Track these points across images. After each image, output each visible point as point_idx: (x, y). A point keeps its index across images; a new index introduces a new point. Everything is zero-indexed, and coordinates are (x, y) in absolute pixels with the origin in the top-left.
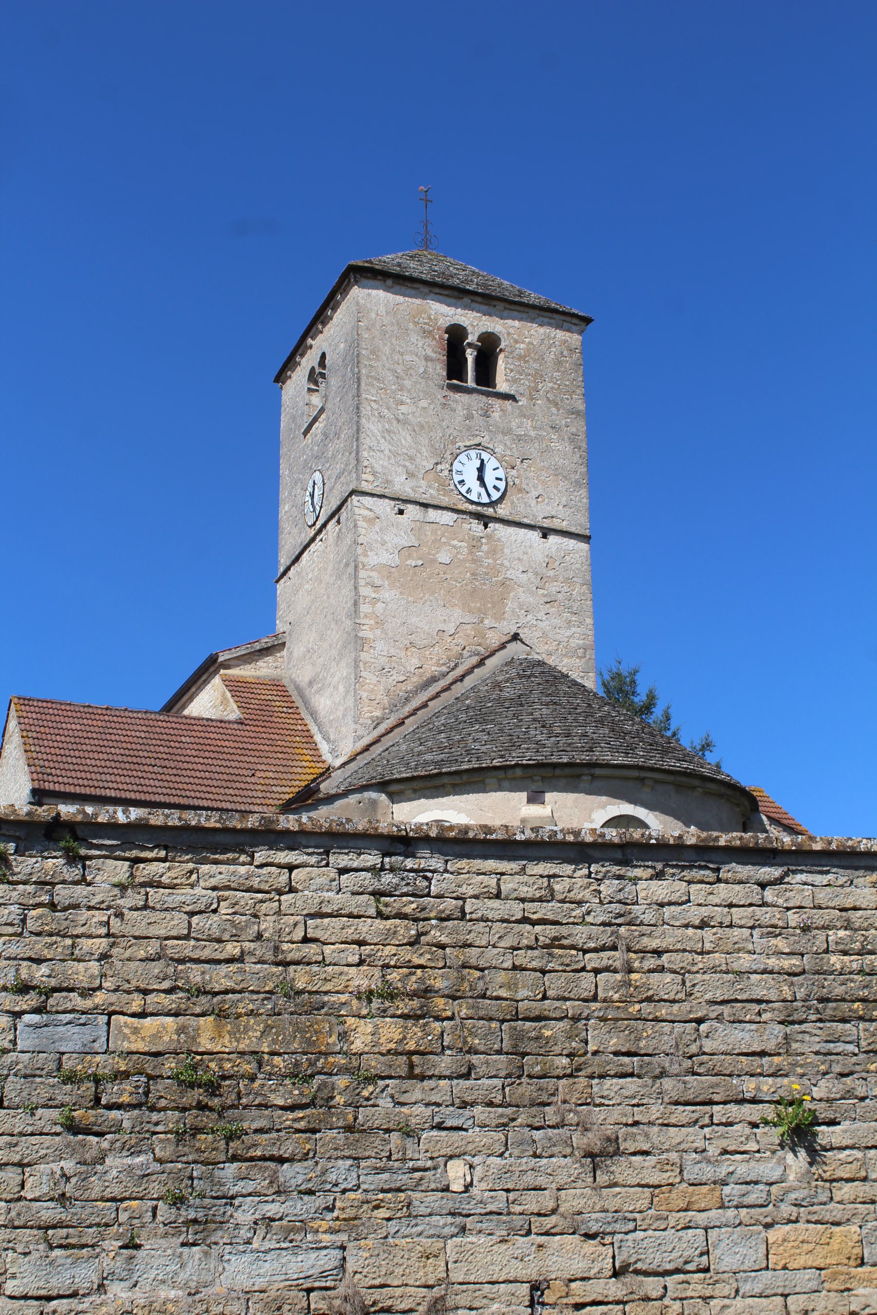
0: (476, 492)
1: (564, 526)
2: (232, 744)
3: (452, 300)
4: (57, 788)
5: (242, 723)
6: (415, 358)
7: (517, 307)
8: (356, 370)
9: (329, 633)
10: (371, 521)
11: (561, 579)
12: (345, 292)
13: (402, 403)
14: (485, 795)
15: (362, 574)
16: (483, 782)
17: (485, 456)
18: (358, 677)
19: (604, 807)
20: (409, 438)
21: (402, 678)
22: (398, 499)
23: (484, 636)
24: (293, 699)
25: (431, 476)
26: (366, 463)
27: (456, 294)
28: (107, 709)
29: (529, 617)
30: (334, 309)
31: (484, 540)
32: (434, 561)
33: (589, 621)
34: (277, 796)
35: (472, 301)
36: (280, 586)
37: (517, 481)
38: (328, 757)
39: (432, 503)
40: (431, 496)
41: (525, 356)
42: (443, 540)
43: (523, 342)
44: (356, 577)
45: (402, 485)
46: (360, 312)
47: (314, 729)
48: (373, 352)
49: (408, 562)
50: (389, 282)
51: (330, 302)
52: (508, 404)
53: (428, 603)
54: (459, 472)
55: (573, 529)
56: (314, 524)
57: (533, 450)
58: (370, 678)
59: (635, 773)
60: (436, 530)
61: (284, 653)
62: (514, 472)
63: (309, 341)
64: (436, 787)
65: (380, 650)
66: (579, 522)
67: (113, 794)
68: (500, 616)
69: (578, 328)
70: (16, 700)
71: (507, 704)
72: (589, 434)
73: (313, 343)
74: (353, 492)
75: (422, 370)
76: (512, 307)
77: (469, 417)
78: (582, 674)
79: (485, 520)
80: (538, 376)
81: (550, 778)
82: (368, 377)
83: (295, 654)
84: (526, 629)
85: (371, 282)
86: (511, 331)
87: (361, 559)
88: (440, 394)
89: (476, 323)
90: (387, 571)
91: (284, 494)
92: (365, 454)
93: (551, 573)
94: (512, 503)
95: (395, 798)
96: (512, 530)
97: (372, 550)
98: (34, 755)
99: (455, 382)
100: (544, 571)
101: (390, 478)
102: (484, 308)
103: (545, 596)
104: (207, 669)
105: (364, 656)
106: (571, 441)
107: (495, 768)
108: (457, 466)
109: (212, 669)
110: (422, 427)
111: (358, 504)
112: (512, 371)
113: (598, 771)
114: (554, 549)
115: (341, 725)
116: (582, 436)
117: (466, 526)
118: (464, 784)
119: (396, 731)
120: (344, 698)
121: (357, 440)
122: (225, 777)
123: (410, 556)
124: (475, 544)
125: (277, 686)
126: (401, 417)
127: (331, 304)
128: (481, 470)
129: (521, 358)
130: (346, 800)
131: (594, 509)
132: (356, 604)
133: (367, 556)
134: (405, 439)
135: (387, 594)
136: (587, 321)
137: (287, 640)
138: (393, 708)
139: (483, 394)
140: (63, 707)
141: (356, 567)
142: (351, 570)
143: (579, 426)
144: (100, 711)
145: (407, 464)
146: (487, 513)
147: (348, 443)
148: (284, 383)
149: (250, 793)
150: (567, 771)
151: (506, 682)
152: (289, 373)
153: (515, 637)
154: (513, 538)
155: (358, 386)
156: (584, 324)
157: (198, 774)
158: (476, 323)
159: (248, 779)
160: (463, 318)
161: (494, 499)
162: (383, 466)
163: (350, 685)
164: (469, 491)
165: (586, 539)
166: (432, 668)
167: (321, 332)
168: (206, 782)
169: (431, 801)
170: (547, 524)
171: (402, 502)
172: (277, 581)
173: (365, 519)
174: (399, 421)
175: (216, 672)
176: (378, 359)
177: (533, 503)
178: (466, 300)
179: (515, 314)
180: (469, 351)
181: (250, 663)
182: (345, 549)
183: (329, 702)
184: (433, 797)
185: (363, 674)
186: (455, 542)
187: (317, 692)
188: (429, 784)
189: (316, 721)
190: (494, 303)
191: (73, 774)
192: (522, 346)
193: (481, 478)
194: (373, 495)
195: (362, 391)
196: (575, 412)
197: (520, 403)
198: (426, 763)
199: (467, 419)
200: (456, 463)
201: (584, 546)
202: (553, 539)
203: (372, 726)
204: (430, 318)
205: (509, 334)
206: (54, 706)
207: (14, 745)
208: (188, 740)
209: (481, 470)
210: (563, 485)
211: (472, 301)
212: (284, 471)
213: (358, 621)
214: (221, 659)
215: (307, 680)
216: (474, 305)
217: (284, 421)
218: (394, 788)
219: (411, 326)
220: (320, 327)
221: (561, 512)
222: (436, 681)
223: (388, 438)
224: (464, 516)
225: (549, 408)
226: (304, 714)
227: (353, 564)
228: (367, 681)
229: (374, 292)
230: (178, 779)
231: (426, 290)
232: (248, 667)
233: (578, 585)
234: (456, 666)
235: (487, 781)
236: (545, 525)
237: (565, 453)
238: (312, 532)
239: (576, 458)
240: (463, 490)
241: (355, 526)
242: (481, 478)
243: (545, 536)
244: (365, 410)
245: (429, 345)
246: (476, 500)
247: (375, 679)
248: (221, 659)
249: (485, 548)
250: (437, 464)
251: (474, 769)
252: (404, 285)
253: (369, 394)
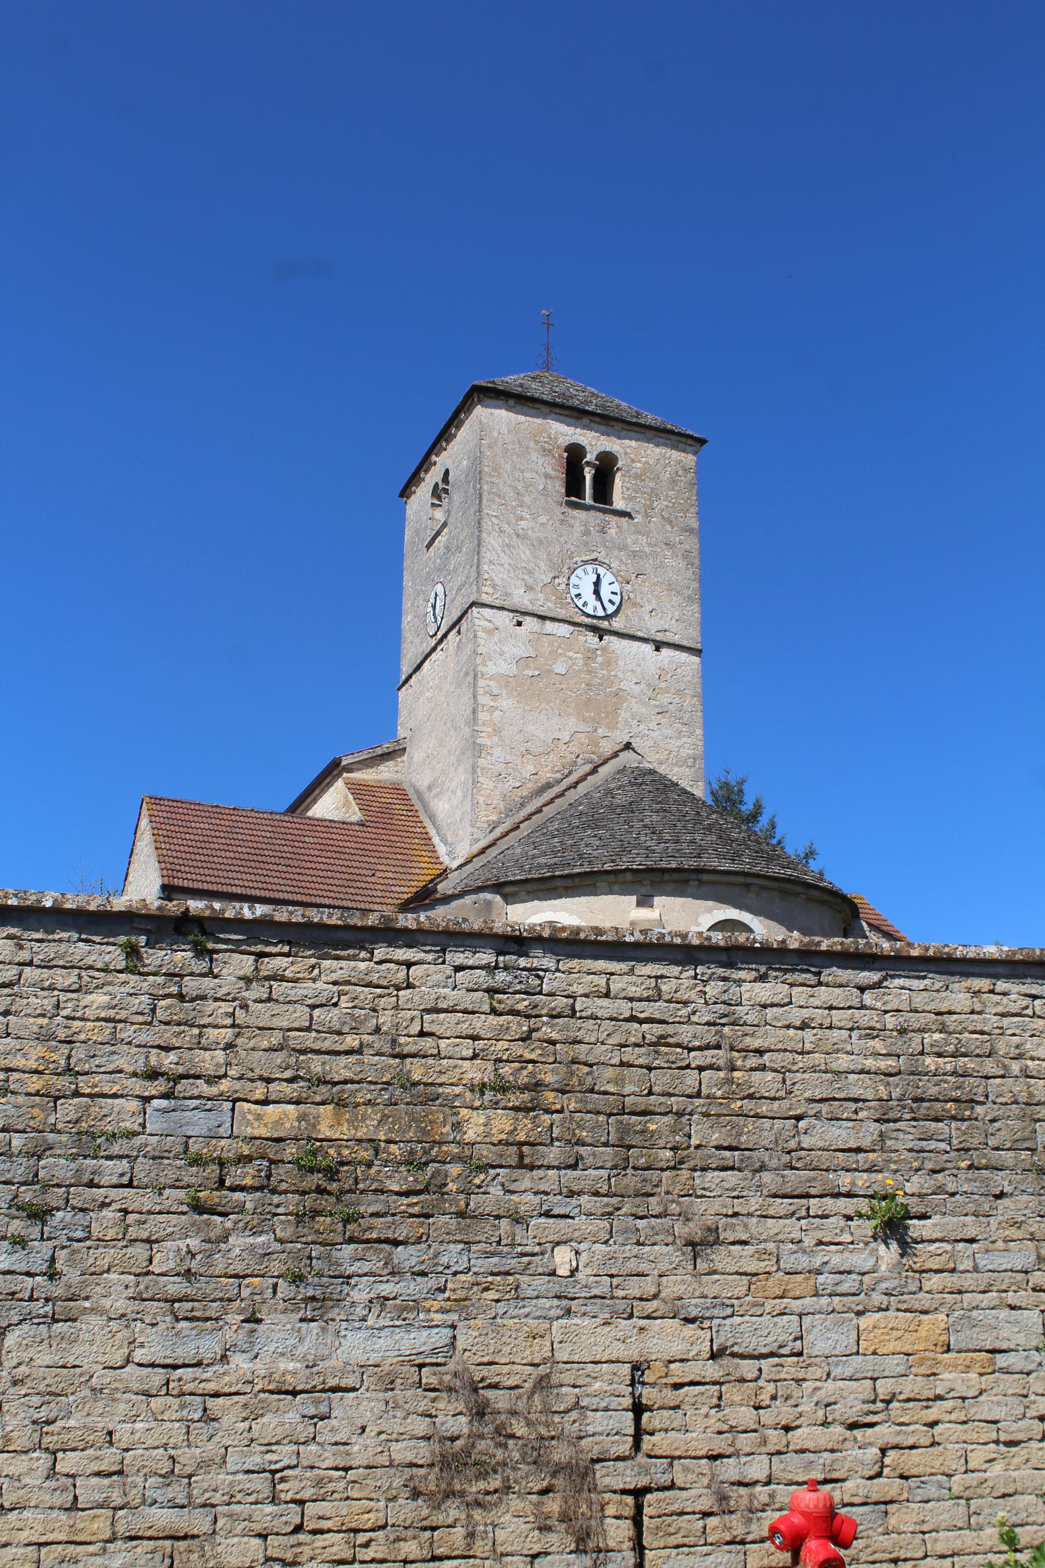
0: (592, 606)
1: (676, 639)
2: (353, 845)
3: (572, 420)
4: (186, 884)
5: (363, 825)
6: (535, 475)
7: (633, 428)
8: (478, 486)
9: (448, 739)
10: (490, 632)
11: (672, 690)
12: (469, 411)
13: (522, 519)
14: (596, 898)
15: (481, 683)
16: (594, 885)
17: (601, 571)
18: (475, 782)
19: (710, 911)
20: (528, 553)
21: (518, 784)
22: (517, 611)
23: (597, 745)
24: (413, 802)
25: (548, 589)
26: (486, 576)
27: (575, 414)
28: (234, 809)
29: (642, 727)
31: (599, 652)
32: (550, 671)
33: (699, 732)
34: (396, 895)
35: (591, 421)
37: (632, 596)
38: (445, 859)
39: (550, 615)
40: (549, 609)
41: (642, 475)
42: (560, 651)
43: (640, 461)
44: (475, 686)
45: (520, 598)
46: (483, 431)
47: (432, 832)
48: (494, 469)
49: (526, 672)
50: (511, 402)
51: (455, 421)
52: (624, 521)
53: (544, 712)
54: (576, 586)
55: (685, 643)
56: (436, 634)
57: (648, 565)
58: (487, 783)
59: (741, 879)
60: (553, 641)
61: (405, 758)
62: (629, 587)
63: (434, 458)
64: (549, 890)
65: (497, 756)
66: (691, 636)
67: (239, 891)
68: (613, 726)
70: (148, 800)
71: (618, 811)
72: (702, 551)
73: (437, 459)
74: (473, 604)
75: (541, 487)
76: (629, 428)
77: (587, 533)
78: (691, 783)
79: (601, 633)
80: (654, 494)
81: (659, 882)
82: (489, 493)
83: (415, 759)
84: (638, 739)
85: (494, 402)
86: (629, 450)
87: (480, 668)
88: (559, 510)
89: (594, 442)
90: (505, 680)
91: (407, 605)
92: (486, 567)
93: (663, 685)
94: (627, 616)
95: (508, 899)
96: (626, 643)
97: (490, 660)
98: (165, 852)
99: (573, 499)
100: (657, 683)
101: (509, 591)
102: (602, 428)
103: (657, 707)
104: (331, 773)
105: (481, 762)
106: (685, 557)
107: (606, 872)
108: (574, 580)
109: (335, 773)
110: (541, 542)
111: (477, 615)
112: (628, 489)
113: (705, 877)
114: (666, 662)
115: (458, 829)
116: (695, 553)
117: (582, 638)
118: (576, 887)
119: (511, 835)
121: (478, 553)
122: (346, 876)
123: (527, 667)
124: (590, 655)
125: (398, 790)
126: (521, 532)
127: (455, 423)
128: (597, 584)
129: (637, 476)
130: (462, 900)
131: (706, 625)
132: (474, 711)
133: (485, 665)
134: (525, 553)
135: (505, 703)
136: (702, 442)
137: (408, 745)
138: (509, 812)
140: (192, 807)
141: (475, 676)
142: (470, 678)
143: (692, 544)
144: (227, 811)
145: (526, 577)
146: (602, 626)
147: (469, 557)
148: (408, 498)
149: (370, 892)
150: (675, 876)
151: (618, 789)
152: (413, 489)
153: (628, 746)
154: (627, 651)
155: (480, 501)
156: (698, 445)
157: (320, 873)
158: (594, 442)
159: (369, 879)
160: (582, 438)
161: (609, 612)
162: (503, 579)
163: (468, 790)
164: (585, 604)
165: (697, 652)
166: (547, 776)
167: (445, 449)
168: (327, 881)
169: (544, 903)
170: (660, 637)
171: (520, 614)
172: (399, 689)
173: (484, 630)
174: (518, 536)
175: (339, 775)
176: (499, 476)
177: (647, 617)
178: (586, 420)
179: (633, 434)
180: (587, 469)
182: (465, 659)
183: (447, 806)
184: (546, 900)
186: (571, 654)
187: (436, 796)
188: (542, 887)
189: (434, 824)
190: (612, 423)
191: (202, 871)
192: (638, 465)
193: (597, 593)
194: (492, 607)
195: (484, 507)
196: (689, 530)
197: (636, 520)
198: (540, 866)
199: (584, 534)
200: (573, 577)
201: (696, 660)
202: (665, 652)
204: (550, 437)
205: (626, 453)
206: (184, 805)
207: (144, 843)
208: (311, 840)
209: (597, 584)
210: (676, 600)
211: (591, 421)
212: (407, 582)
213: (476, 728)
214: (344, 763)
215: (426, 784)
216: (593, 425)
218: (508, 890)
219: (532, 444)
221: (674, 626)
223: (508, 552)
225: (663, 526)
226: (423, 817)
227: (472, 673)
229: (497, 412)
230: (301, 877)
231: (545, 409)
232: (370, 771)
233: (689, 698)
234: (570, 773)
235: (598, 884)
236: (658, 639)
237: (678, 569)
238: (434, 642)
239: (689, 574)
240: (580, 603)
241: (475, 636)
242: (597, 593)
243: (657, 649)
244: (486, 525)
245: (549, 464)
246: (592, 613)
247: (491, 785)
248: (344, 763)
249: (600, 659)
250: (554, 578)
251: (586, 873)
253: (490, 509)
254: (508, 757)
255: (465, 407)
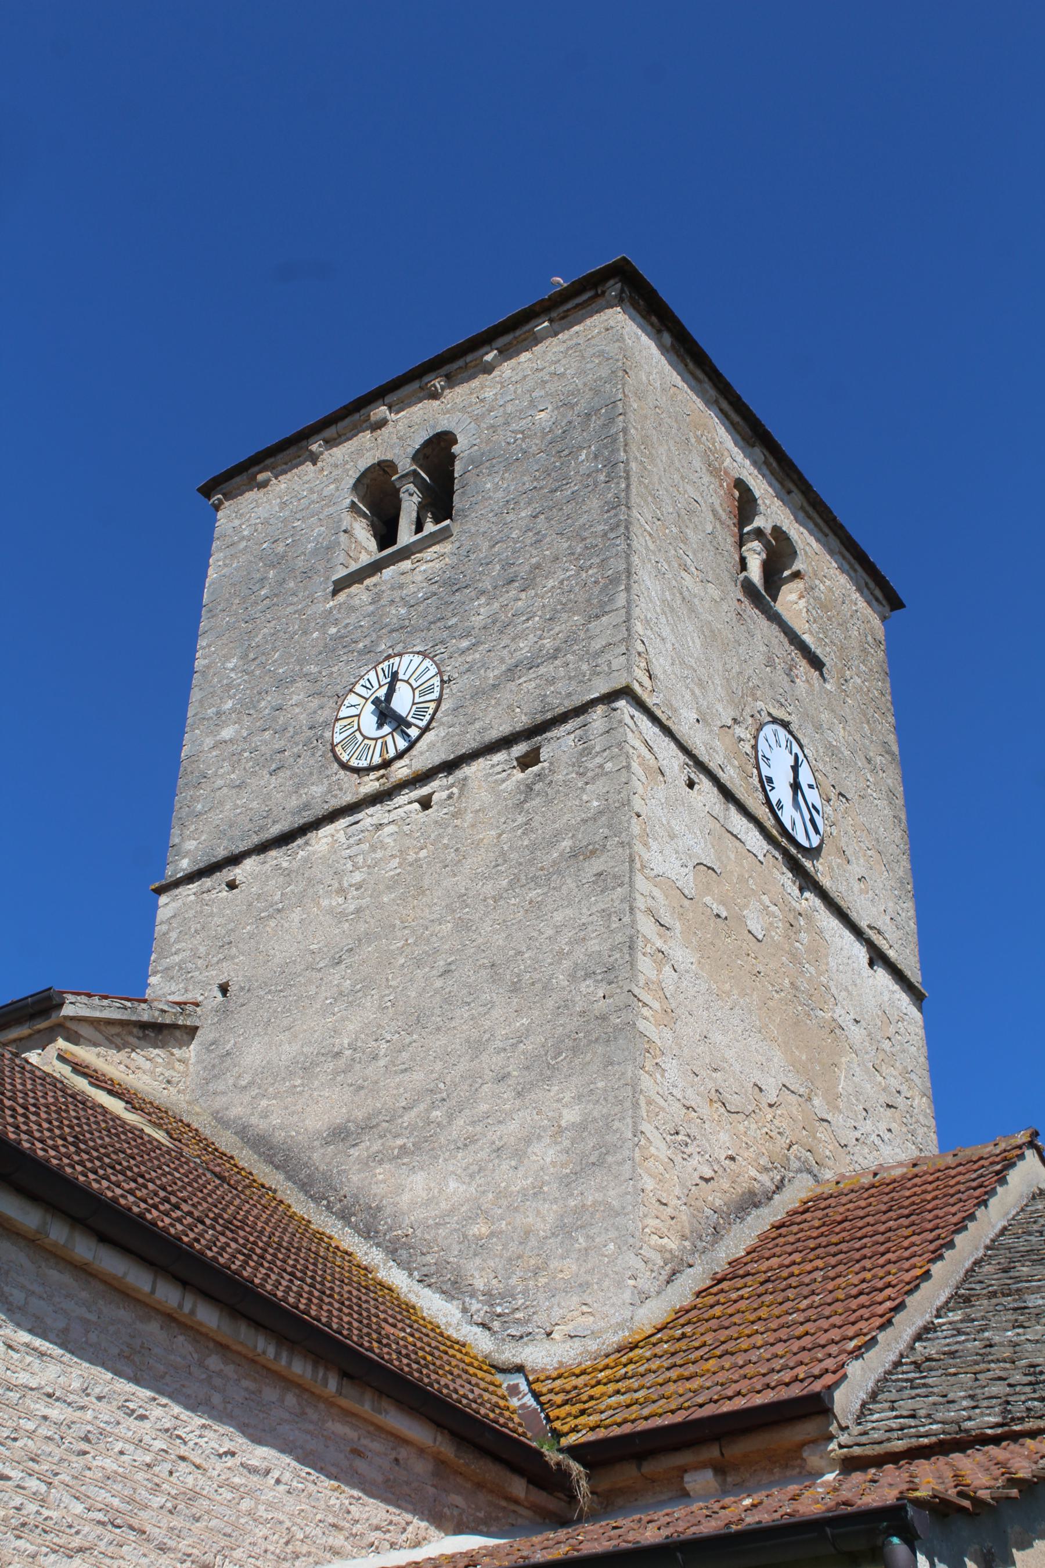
20: (697, 641)
21: (709, 1174)
26: (641, 648)
30: (507, 353)
32: (742, 919)
36: (167, 905)
51: (511, 332)
56: (386, 764)
61: (192, 1051)
63: (381, 411)
69: (880, 608)
73: (393, 416)
83: (253, 1055)
120: (567, 1182)
121: (628, 589)
127: (501, 341)
135: (682, 955)
139: (785, 633)
143: (892, 778)
152: (261, 477)
156: (887, 608)
172: (160, 891)
181: (119, 1049)
185: (646, 1127)
189: (368, 1233)
197: (828, 686)
203: (664, 1277)
214: (67, 1010)
217: (218, 569)
220: (438, 383)
222: (756, 1206)
224: (777, 854)
228: (653, 1150)
229: (644, 338)
238: (370, 785)
248: (67, 1010)
252: (683, 361)
254: (689, 1092)
255: (567, 305)
